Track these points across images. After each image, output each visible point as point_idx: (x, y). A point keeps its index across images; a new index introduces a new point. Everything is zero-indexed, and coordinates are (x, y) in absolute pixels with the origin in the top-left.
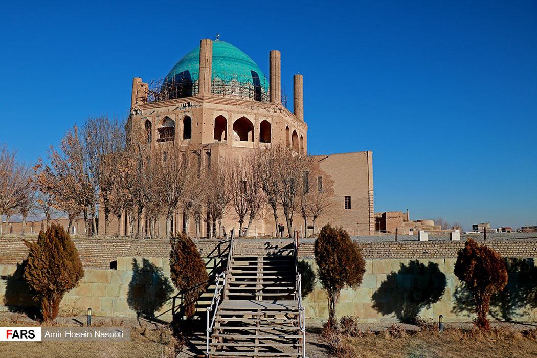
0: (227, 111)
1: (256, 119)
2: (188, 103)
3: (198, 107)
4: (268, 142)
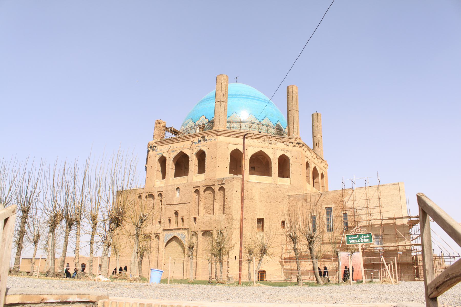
2: (203, 137)
3: (213, 141)
4: (287, 177)
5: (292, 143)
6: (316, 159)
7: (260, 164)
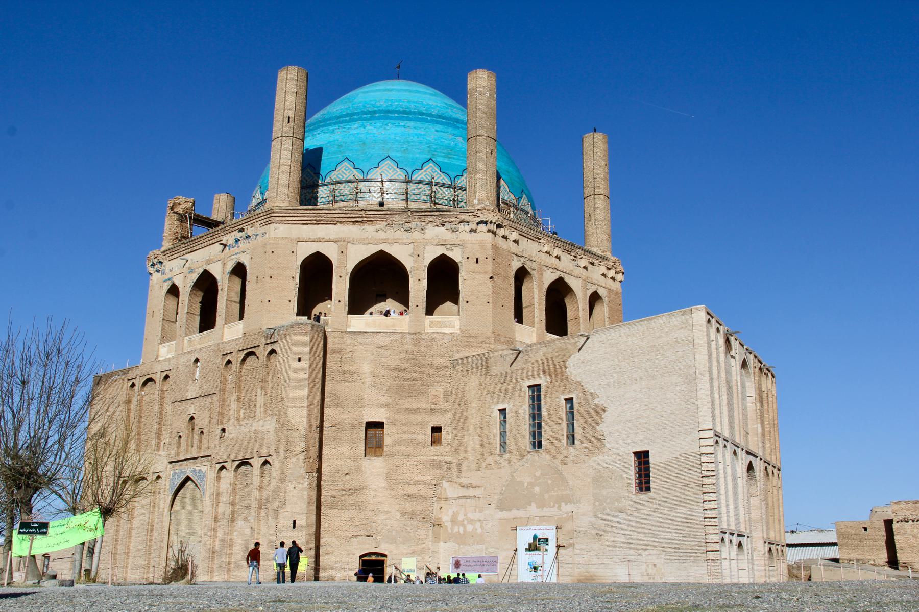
0: (336, 242)
6: (566, 258)
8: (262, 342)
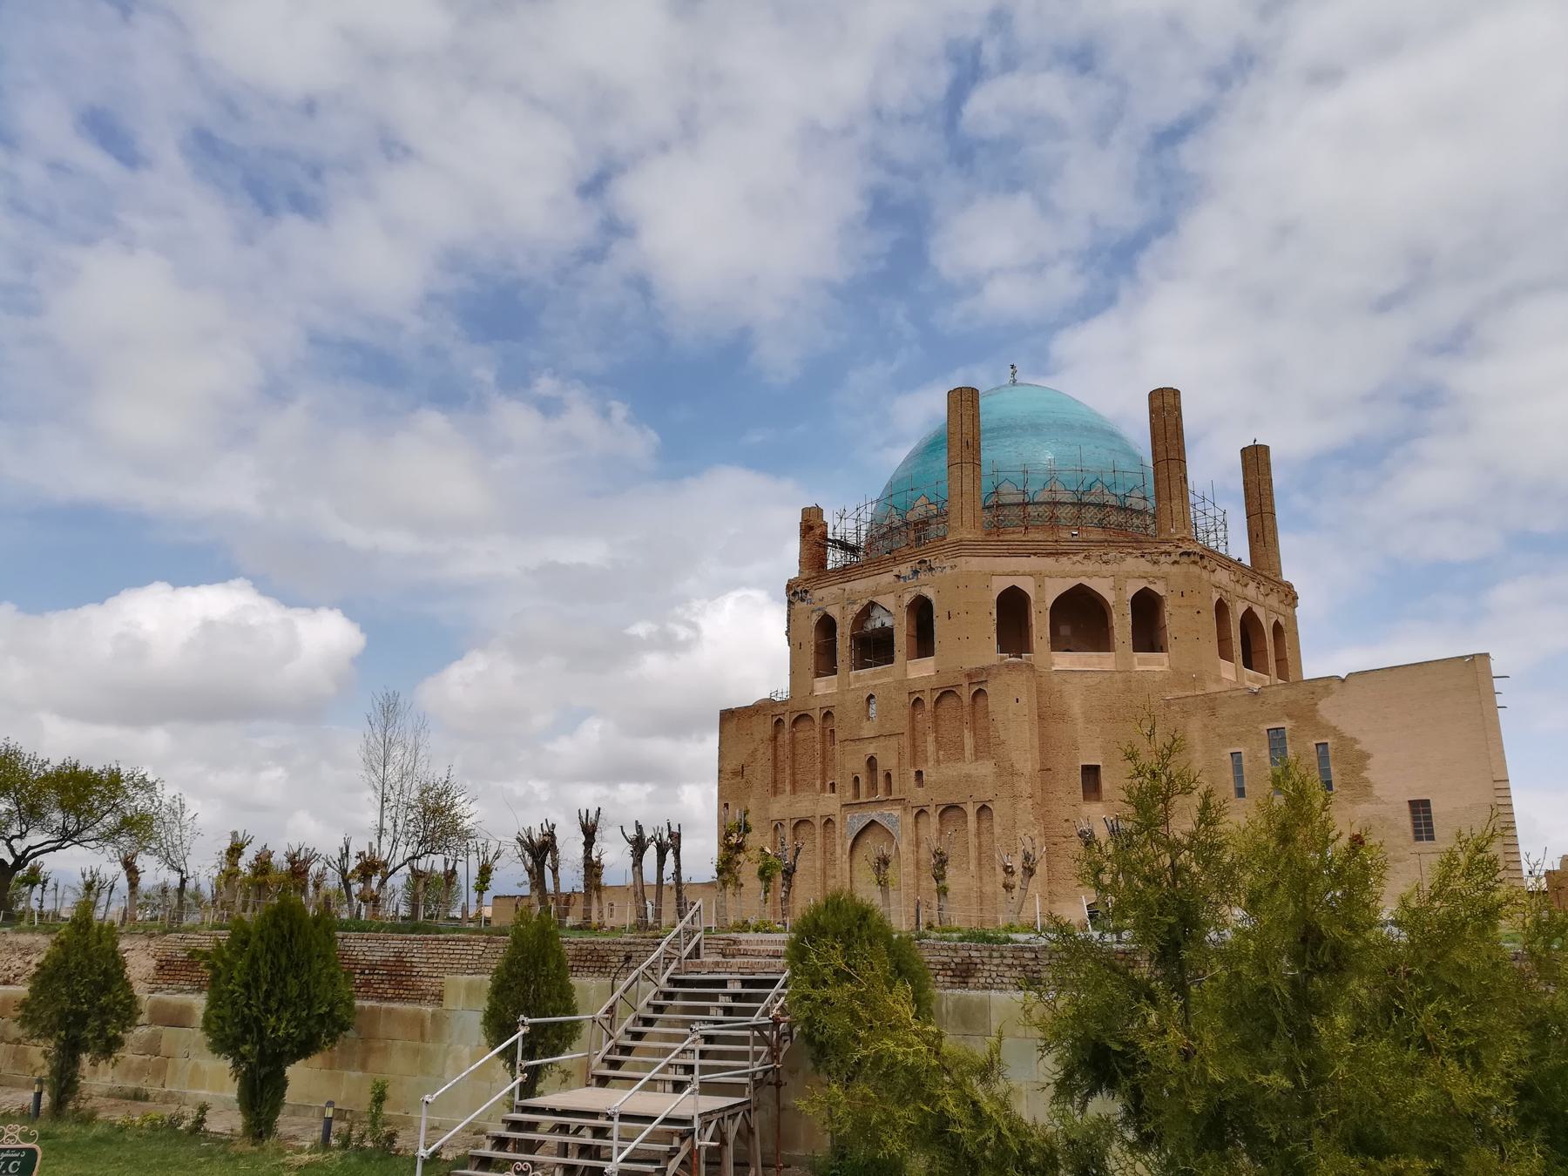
1: (1118, 589)
3: (948, 571)
5: (1169, 554)
7: (1081, 618)
8: (966, 684)
